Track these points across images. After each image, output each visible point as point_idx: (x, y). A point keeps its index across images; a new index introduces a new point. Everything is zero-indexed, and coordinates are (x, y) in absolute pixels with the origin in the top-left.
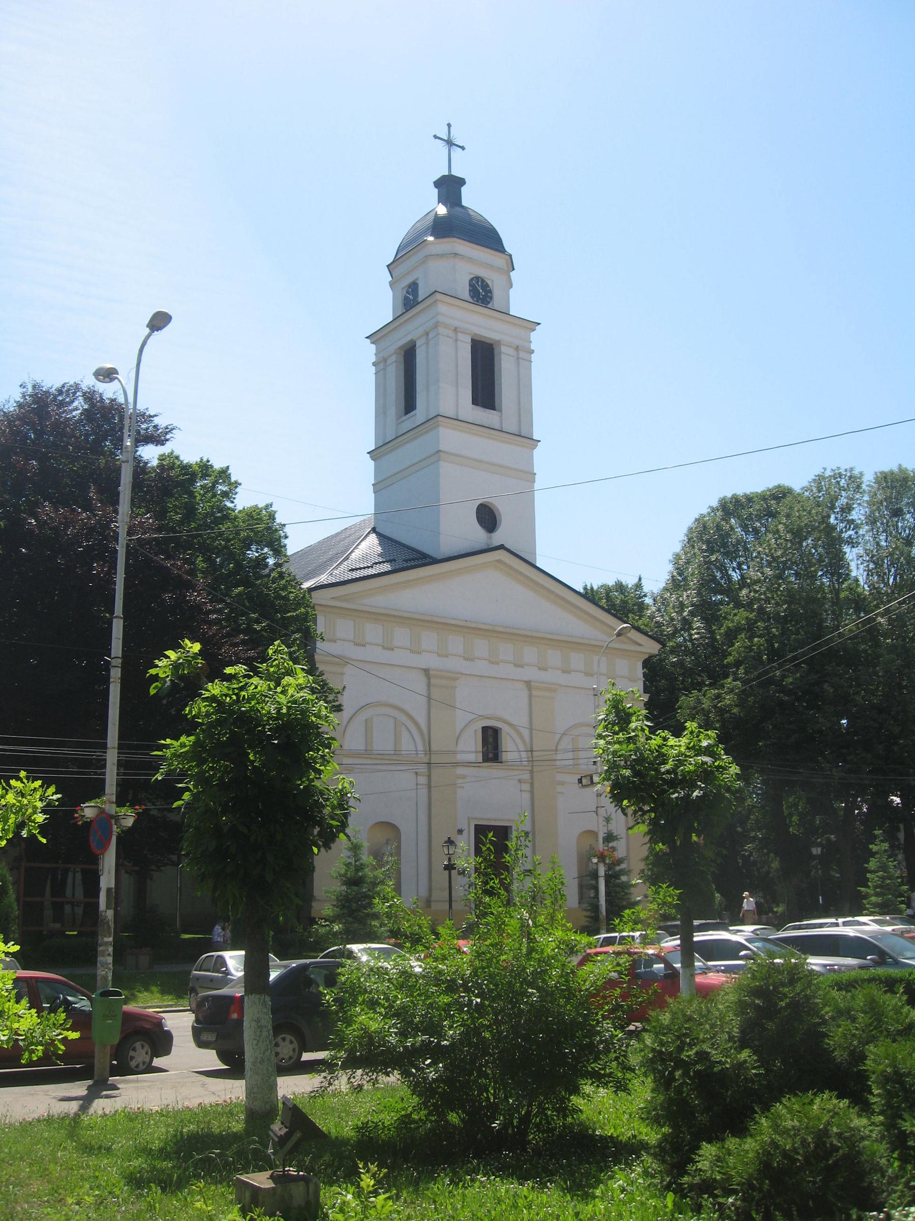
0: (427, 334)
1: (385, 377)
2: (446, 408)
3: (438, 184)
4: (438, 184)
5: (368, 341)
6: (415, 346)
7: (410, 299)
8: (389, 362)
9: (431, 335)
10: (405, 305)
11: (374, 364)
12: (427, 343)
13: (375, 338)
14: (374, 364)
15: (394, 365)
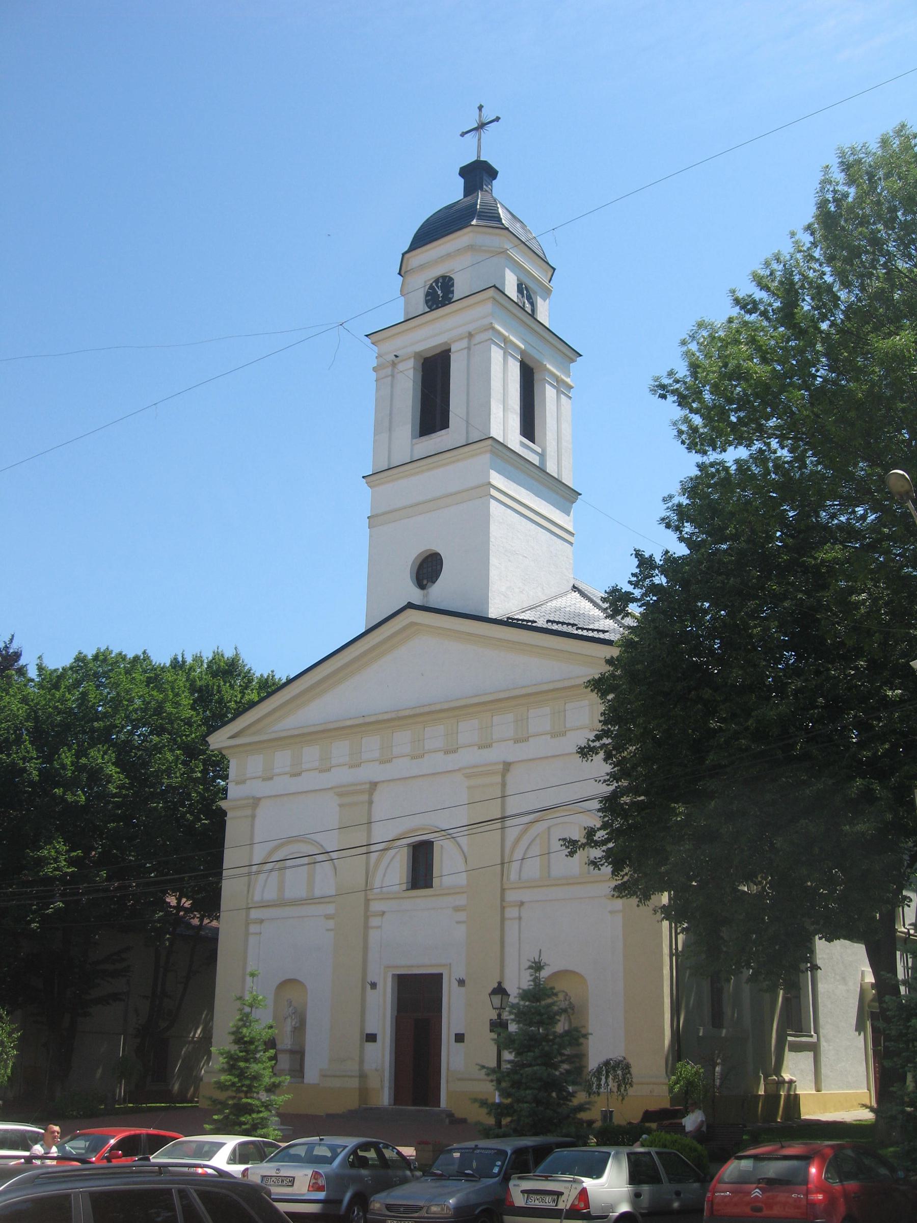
0: (470, 335)
1: (392, 386)
2: (496, 432)
3: (465, 172)
4: (465, 172)
5: (368, 341)
6: (449, 350)
7: (440, 294)
8: (401, 367)
9: (477, 339)
10: (427, 302)
11: (375, 369)
12: (469, 348)
13: (375, 337)
14: (375, 369)
15: (412, 370)
